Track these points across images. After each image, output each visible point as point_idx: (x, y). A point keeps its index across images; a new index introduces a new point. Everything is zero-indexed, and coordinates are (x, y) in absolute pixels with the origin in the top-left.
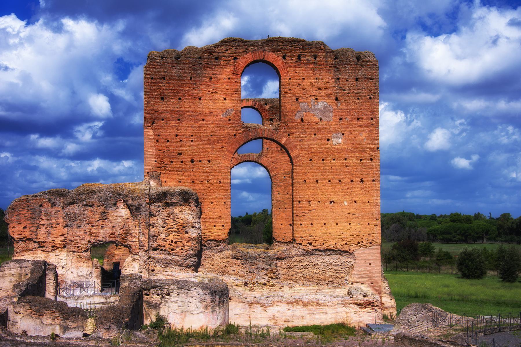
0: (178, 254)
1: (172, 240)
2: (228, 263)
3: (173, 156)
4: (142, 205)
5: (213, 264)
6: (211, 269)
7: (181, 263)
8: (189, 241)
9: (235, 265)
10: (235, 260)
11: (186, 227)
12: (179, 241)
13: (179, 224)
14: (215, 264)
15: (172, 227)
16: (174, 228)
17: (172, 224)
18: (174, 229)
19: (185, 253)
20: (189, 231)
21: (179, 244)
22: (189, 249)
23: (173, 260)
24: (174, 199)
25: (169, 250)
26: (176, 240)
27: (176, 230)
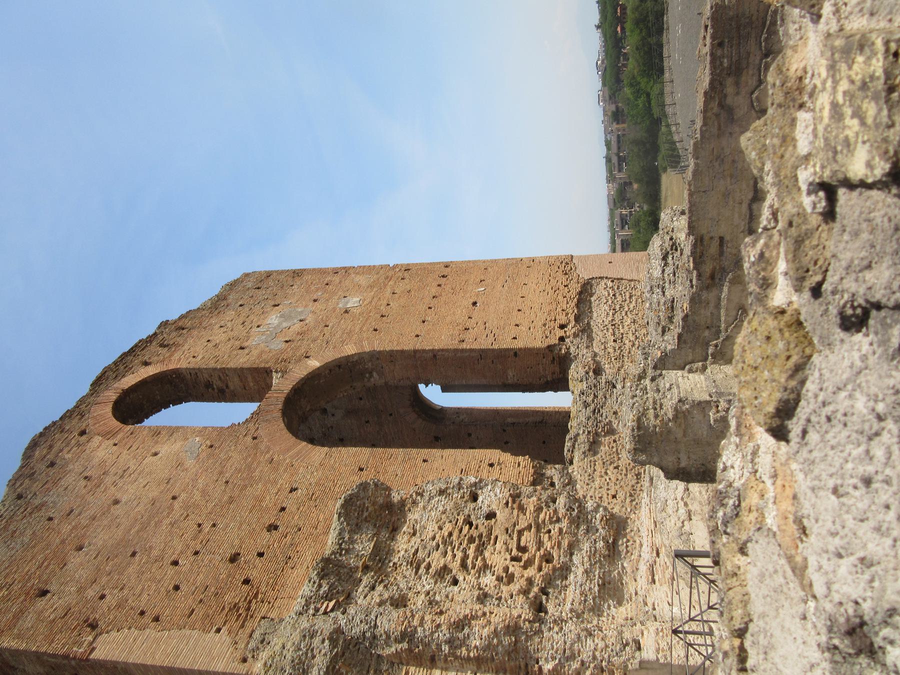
0: (565, 543)
1: (509, 557)
2: (608, 463)
3: (229, 576)
4: (338, 631)
5: (610, 497)
6: (628, 500)
7: (600, 544)
8: (522, 509)
9: (614, 450)
10: (603, 449)
11: (469, 516)
12: (515, 539)
13: (454, 537)
14: (612, 492)
15: (459, 555)
16: (464, 551)
17: (450, 553)
18: (471, 552)
19: (564, 524)
20: (485, 510)
21: (528, 539)
22: (548, 506)
23: (587, 565)
24: (364, 545)
25: (547, 568)
26: (513, 545)
27: (473, 546)
